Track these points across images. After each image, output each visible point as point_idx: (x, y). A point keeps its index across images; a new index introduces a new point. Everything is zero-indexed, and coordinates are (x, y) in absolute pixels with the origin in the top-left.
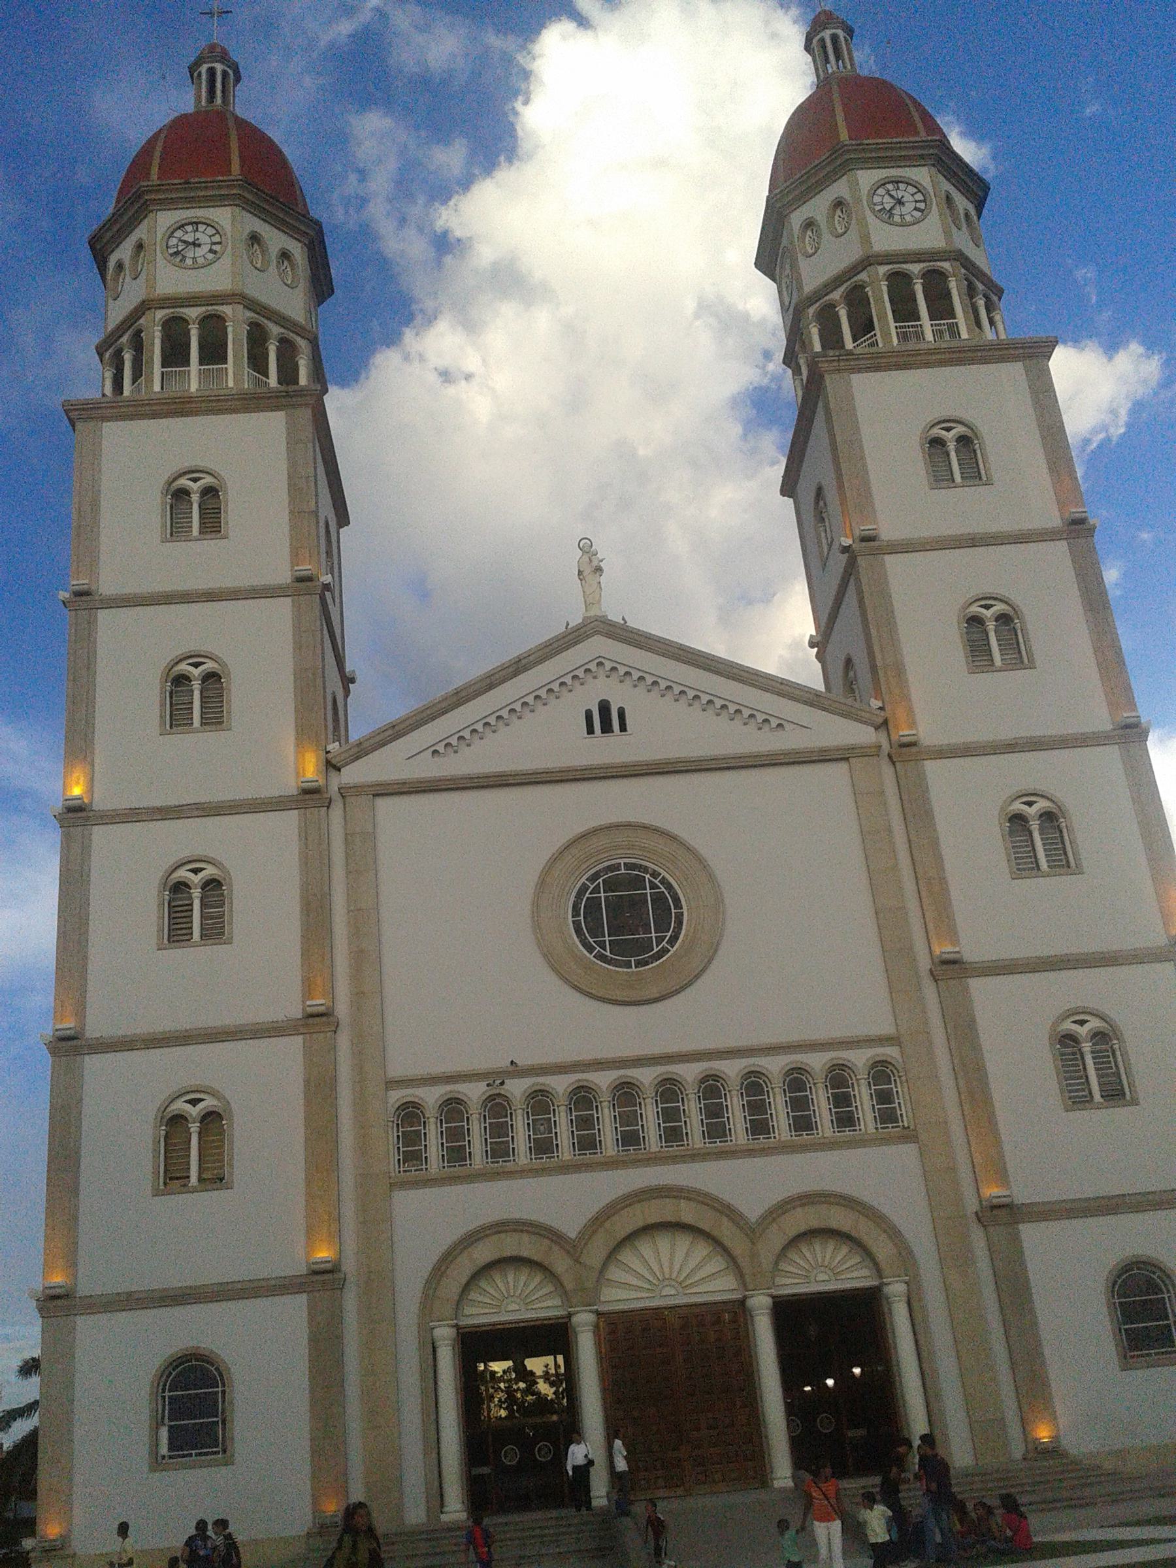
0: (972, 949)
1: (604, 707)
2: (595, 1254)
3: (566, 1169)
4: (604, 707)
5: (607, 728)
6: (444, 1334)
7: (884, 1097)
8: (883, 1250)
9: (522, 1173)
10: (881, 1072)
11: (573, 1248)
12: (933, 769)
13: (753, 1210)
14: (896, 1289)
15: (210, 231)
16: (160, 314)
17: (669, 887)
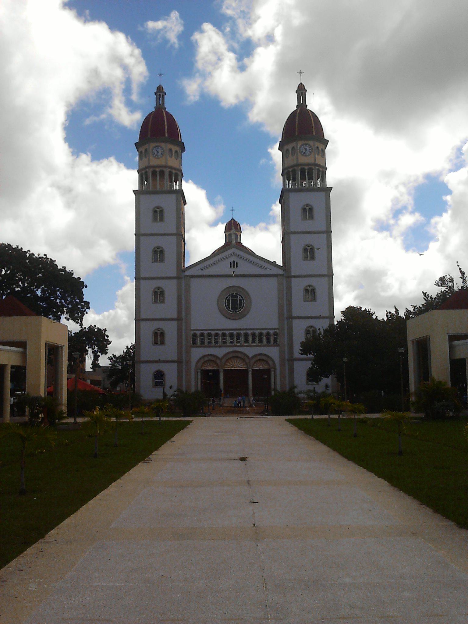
0: (295, 314)
1: (234, 262)
2: (224, 360)
3: (220, 346)
4: (234, 262)
5: (234, 266)
6: (199, 371)
7: (275, 338)
8: (271, 363)
9: (213, 347)
10: (275, 334)
11: (221, 359)
12: (293, 279)
13: (250, 355)
14: (273, 369)
15: (161, 149)
16: (152, 169)
17: (242, 298)
